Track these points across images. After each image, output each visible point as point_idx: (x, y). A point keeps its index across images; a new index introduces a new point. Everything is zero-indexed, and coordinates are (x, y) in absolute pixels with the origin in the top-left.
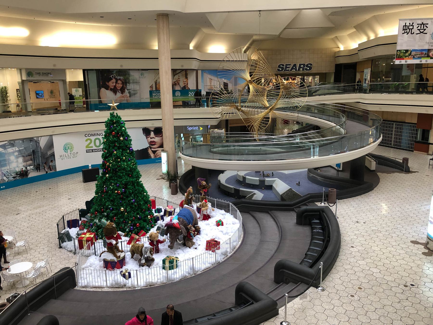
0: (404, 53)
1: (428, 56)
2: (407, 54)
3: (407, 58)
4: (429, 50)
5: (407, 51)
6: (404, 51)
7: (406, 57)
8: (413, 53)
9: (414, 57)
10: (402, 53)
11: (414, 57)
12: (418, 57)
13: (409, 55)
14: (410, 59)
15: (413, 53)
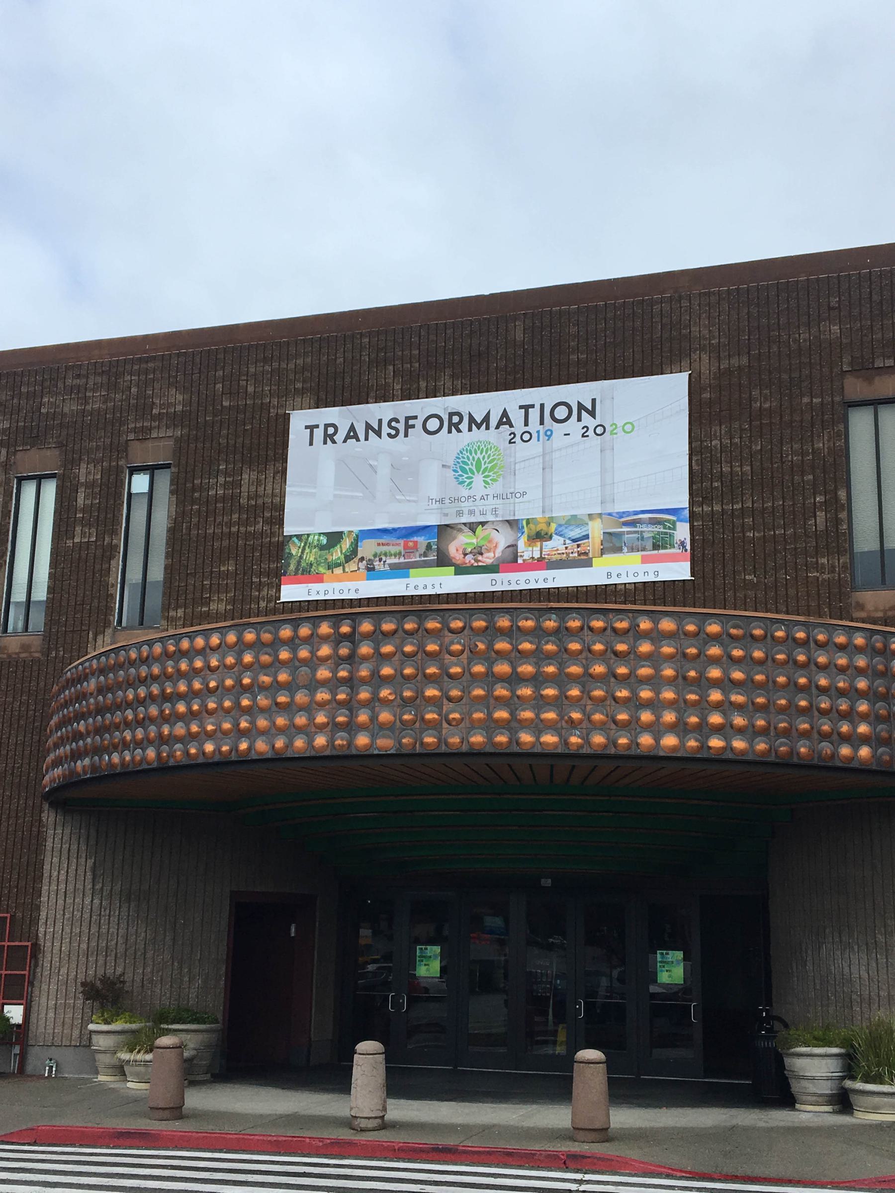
0: (322, 548)
1: (443, 561)
2: (337, 554)
3: (338, 571)
4: (444, 531)
5: (335, 538)
6: (324, 540)
7: (331, 567)
8: (367, 548)
9: (370, 569)
10: (311, 546)
11: (370, 569)
12: (393, 567)
13: (348, 559)
14: (354, 576)
15: (367, 548)
